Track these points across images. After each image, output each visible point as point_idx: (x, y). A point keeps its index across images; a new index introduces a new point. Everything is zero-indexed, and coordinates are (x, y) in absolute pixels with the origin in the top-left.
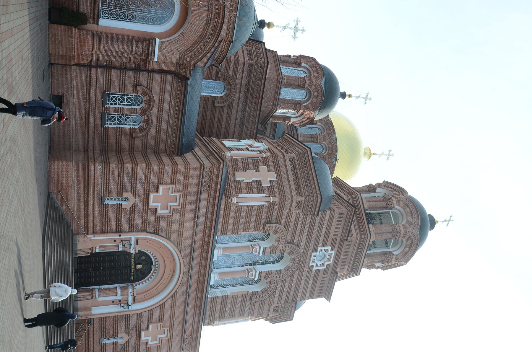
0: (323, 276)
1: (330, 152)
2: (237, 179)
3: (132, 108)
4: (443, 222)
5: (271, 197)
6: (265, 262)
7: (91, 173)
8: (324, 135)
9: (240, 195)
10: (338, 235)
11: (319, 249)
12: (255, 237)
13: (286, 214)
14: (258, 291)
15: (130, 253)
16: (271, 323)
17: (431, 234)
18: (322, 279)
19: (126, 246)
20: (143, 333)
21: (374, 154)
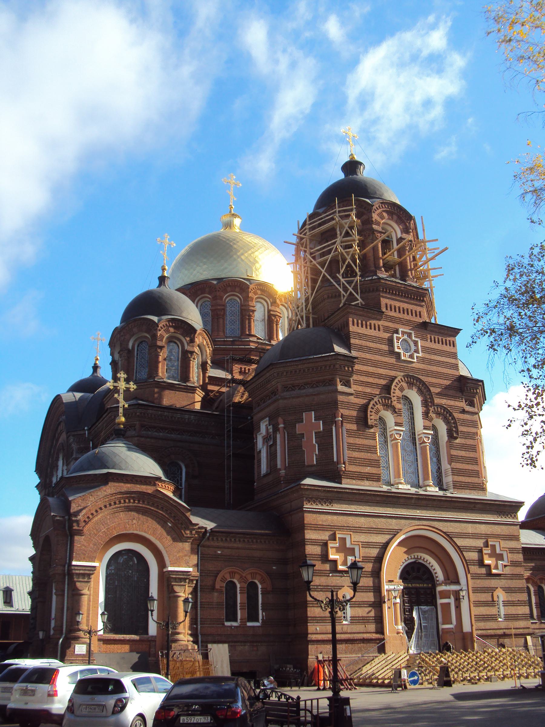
0: (429, 340)
1: (237, 289)
2: (315, 463)
3: (240, 593)
5: (337, 419)
6: (411, 420)
7: (320, 637)
8: (213, 298)
9: (335, 460)
10: (379, 326)
11: (397, 350)
12: (382, 435)
13: (356, 399)
14: (447, 429)
15: (403, 590)
16: (485, 401)
18: (433, 342)
19: (396, 595)
20: (494, 571)
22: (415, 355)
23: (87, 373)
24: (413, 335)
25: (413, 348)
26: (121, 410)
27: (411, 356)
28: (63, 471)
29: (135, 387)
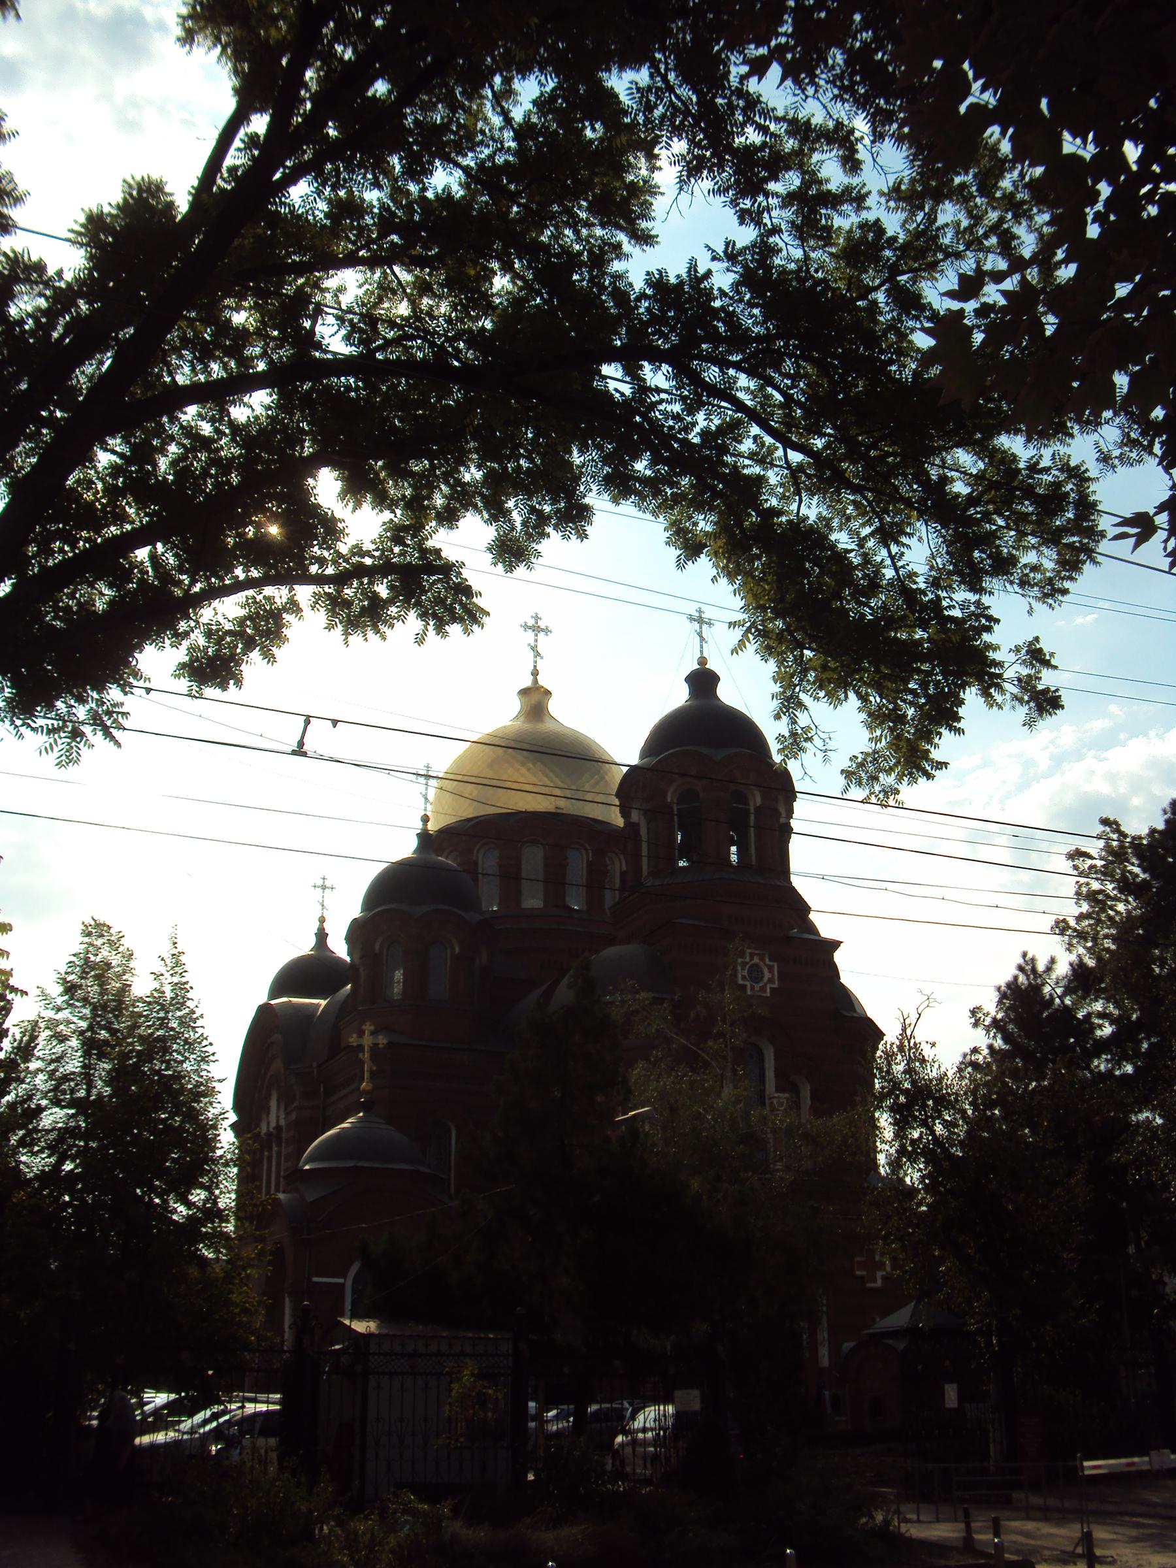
4: (702, 639)
11: (740, 982)
17: (727, 694)
20: (870, 1285)
21: (535, 673)
22: (768, 987)
23: (305, 946)
24: (767, 960)
25: (767, 975)
26: (366, 1075)
27: (763, 989)
28: (278, 1117)
29: (385, 1041)
